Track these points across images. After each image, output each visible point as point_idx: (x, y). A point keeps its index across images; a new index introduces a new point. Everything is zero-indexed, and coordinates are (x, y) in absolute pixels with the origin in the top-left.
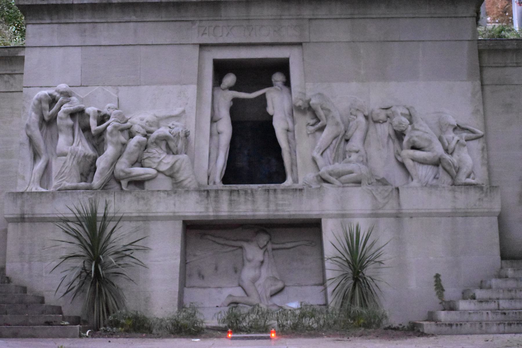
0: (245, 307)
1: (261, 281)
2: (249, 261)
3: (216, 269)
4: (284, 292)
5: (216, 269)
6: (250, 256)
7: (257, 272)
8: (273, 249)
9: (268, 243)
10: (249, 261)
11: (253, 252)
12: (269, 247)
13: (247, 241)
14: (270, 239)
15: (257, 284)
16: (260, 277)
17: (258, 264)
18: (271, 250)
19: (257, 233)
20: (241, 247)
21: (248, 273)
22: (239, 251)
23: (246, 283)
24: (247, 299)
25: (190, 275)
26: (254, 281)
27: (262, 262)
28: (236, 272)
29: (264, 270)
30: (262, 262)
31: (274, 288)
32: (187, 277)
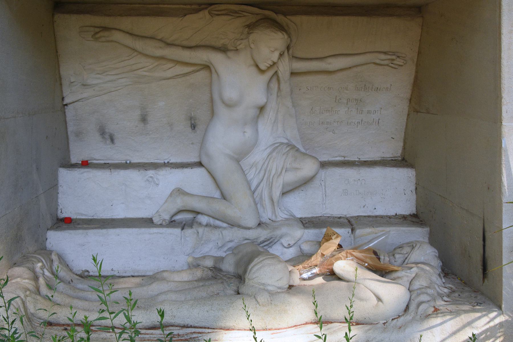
0: (216, 227)
1: (258, 156)
2: (229, 105)
3: (144, 119)
4: (317, 182)
5: (144, 119)
6: (230, 93)
7: (249, 132)
8: (293, 74)
9: (281, 55)
10: (229, 105)
11: (239, 80)
12: (285, 67)
13: (223, 50)
14: (288, 48)
15: (246, 163)
16: (255, 143)
17: (252, 112)
18: (288, 74)
19: (251, 27)
20: (207, 67)
21: (224, 137)
22: (203, 74)
23: (221, 164)
24: (220, 207)
25: (78, 134)
26: (238, 158)
27: (262, 109)
28: (194, 127)
29: (267, 133)
30: (262, 109)
31: (290, 177)
32: (72, 138)
